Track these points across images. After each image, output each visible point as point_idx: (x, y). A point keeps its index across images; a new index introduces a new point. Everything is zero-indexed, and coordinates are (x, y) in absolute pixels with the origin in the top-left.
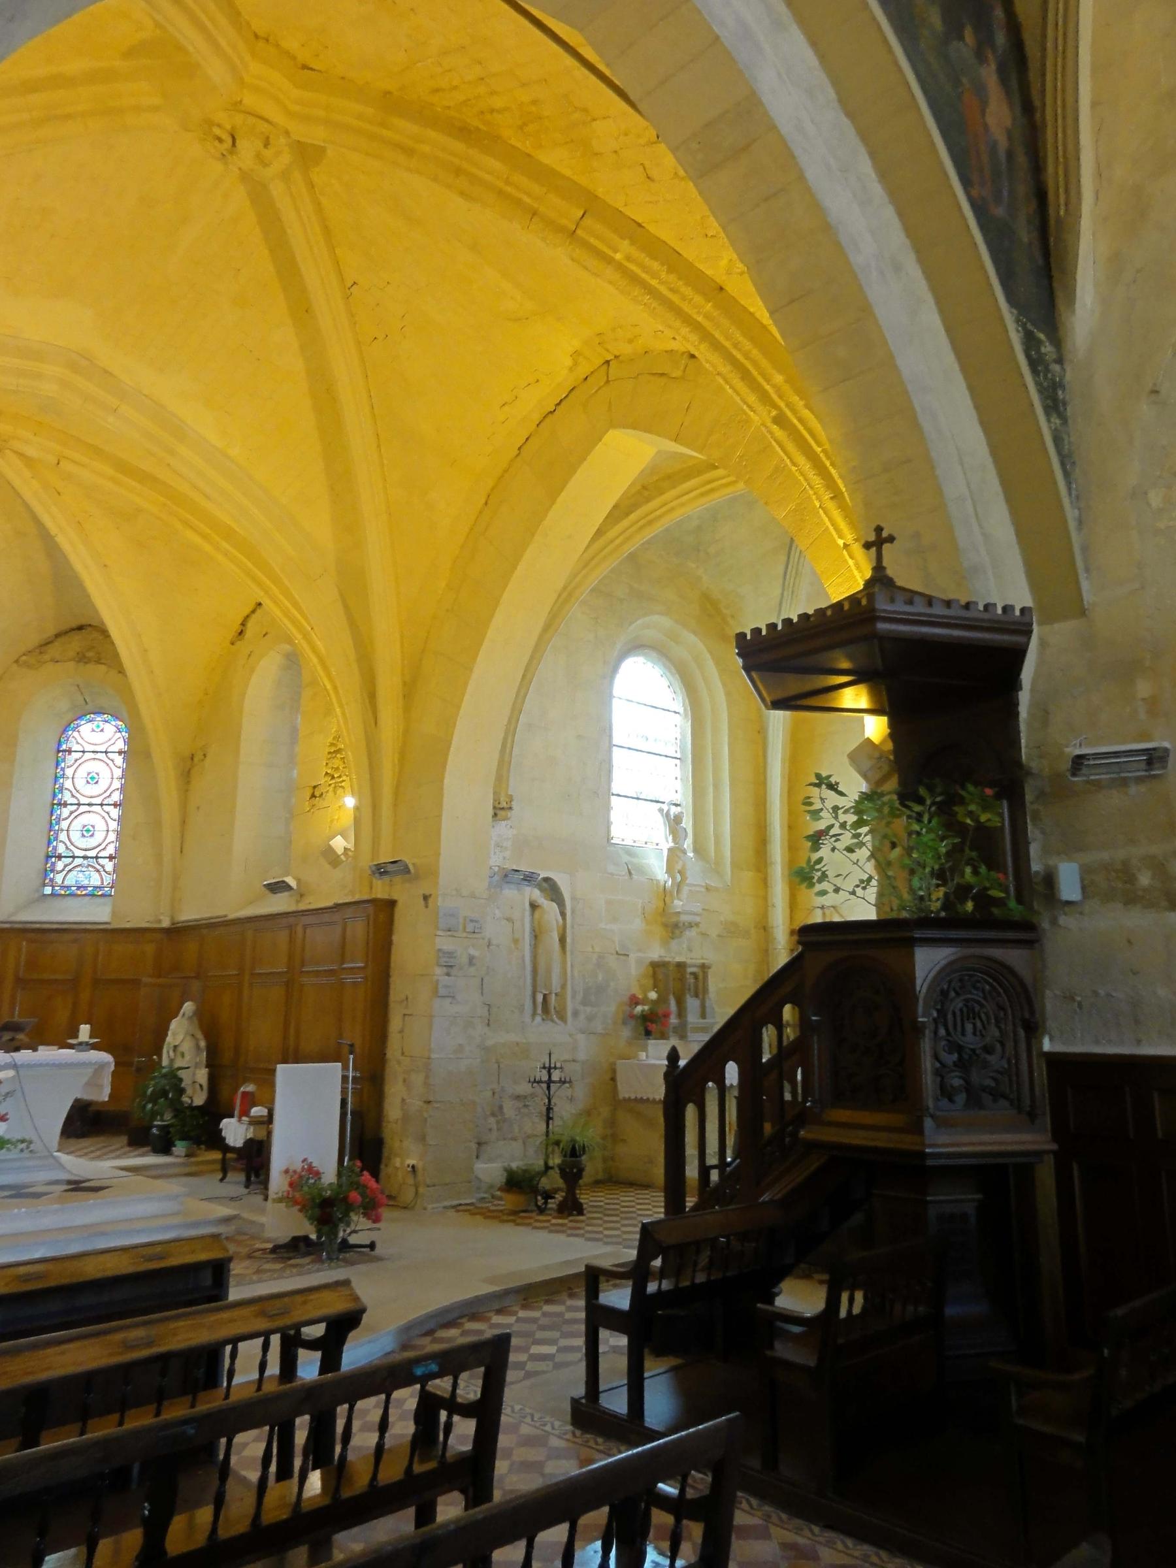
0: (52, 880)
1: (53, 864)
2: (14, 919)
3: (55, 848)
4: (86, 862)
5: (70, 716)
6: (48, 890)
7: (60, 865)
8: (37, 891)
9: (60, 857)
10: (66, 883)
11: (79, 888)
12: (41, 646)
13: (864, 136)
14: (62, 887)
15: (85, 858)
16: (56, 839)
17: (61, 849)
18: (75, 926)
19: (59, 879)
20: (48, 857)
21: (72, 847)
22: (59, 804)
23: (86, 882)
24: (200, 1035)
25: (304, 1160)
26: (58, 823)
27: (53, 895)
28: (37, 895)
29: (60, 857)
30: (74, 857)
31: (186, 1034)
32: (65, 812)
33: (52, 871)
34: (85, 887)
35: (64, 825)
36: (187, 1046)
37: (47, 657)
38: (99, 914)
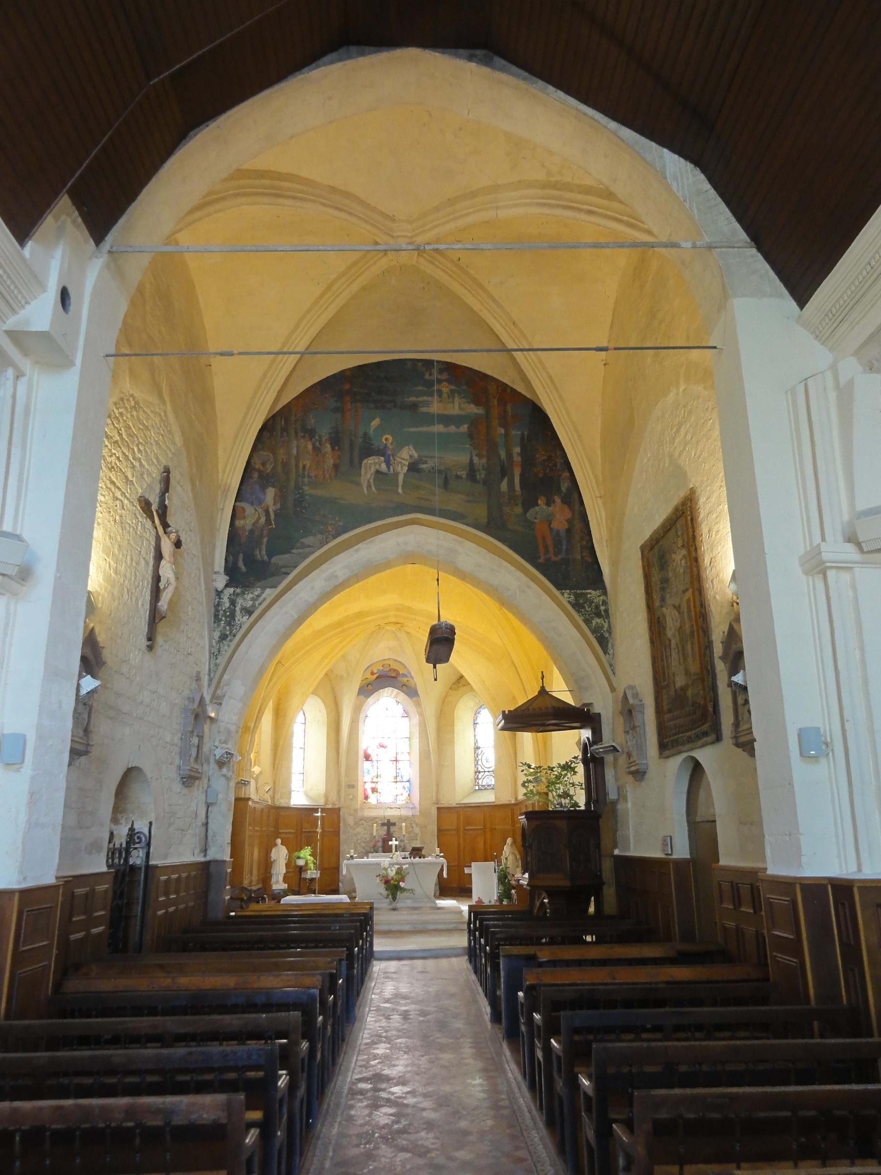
0: (478, 783)
1: (478, 776)
2: (462, 802)
3: (478, 768)
4: (489, 774)
5: (476, 708)
6: (477, 788)
7: (480, 776)
8: (472, 788)
9: (480, 772)
10: (484, 783)
11: (488, 786)
12: (459, 680)
13: (499, 556)
14: (482, 786)
15: (489, 772)
16: (477, 764)
17: (480, 769)
18: (482, 804)
19: (480, 782)
20: (476, 772)
21: (483, 767)
22: (477, 748)
23: (490, 783)
24: (516, 853)
25: (479, 898)
26: (477, 757)
27: (480, 789)
28: (472, 791)
29: (480, 772)
30: (485, 772)
31: (510, 852)
32: (480, 751)
33: (478, 779)
34: (490, 785)
35: (480, 757)
36: (510, 858)
37: (460, 685)
38: (489, 797)
